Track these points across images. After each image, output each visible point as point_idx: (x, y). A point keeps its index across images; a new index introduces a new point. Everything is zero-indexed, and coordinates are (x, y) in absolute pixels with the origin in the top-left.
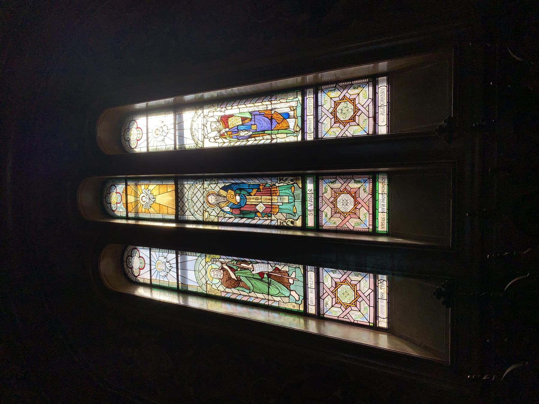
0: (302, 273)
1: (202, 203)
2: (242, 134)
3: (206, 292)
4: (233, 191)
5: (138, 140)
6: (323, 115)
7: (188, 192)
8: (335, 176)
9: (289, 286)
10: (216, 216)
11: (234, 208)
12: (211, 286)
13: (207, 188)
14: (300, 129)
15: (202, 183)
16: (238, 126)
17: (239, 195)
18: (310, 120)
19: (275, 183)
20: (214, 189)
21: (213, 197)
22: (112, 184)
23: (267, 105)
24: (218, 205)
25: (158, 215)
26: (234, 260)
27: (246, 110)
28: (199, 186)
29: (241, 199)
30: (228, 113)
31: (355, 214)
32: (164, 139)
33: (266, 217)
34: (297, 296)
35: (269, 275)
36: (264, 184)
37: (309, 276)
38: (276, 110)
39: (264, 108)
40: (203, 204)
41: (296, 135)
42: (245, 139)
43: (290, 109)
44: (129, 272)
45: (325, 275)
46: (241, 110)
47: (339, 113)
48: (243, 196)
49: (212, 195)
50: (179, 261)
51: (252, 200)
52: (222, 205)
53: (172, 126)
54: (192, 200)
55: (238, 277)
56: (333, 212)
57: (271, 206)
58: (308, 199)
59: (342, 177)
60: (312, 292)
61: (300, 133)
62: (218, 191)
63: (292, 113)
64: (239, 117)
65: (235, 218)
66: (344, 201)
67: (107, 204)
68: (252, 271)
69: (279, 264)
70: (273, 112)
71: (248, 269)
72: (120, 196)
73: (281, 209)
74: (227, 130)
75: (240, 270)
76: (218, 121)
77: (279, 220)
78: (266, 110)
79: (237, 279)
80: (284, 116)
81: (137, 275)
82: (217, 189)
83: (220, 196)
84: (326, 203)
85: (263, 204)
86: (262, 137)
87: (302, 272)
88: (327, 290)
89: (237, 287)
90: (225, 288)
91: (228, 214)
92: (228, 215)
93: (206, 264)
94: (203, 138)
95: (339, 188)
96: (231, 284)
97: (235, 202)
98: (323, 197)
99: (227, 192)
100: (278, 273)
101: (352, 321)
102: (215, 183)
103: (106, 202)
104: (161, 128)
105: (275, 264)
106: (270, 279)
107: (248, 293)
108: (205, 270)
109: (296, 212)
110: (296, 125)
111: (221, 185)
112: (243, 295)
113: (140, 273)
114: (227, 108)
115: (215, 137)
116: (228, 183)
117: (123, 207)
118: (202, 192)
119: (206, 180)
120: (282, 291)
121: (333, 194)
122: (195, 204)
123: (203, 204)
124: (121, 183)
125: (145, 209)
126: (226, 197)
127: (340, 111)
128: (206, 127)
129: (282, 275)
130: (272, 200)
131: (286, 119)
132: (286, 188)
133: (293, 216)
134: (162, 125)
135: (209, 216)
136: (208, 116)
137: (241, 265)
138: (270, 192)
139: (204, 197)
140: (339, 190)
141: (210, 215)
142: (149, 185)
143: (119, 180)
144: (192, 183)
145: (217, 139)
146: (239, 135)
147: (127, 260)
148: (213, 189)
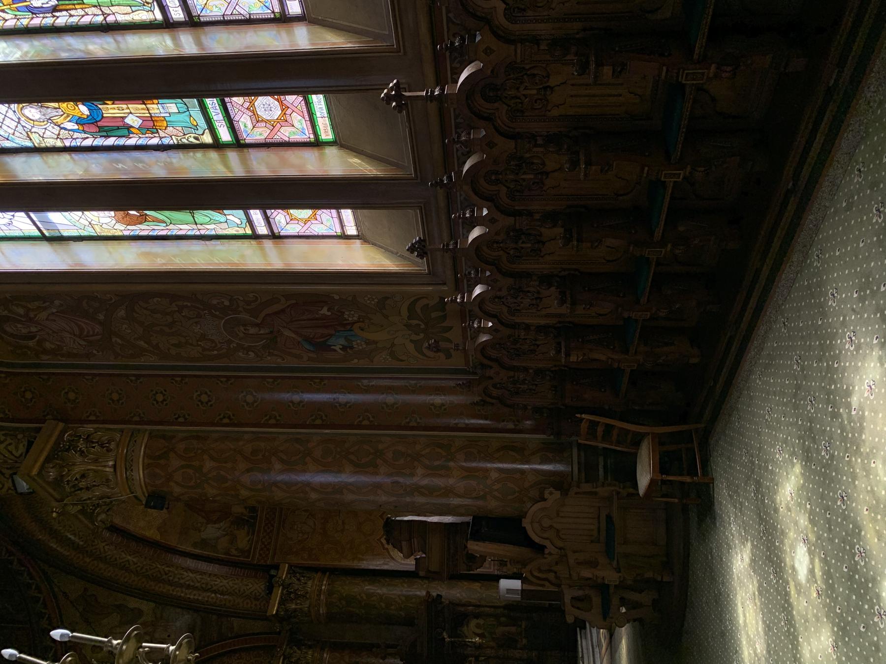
31: (286, 121)
48: (91, 106)
58: (210, 106)
77: (173, 137)
85: (137, 116)
90: (125, 226)
92: (76, 135)
101: (317, 234)
126: (60, 108)
141: (43, 137)
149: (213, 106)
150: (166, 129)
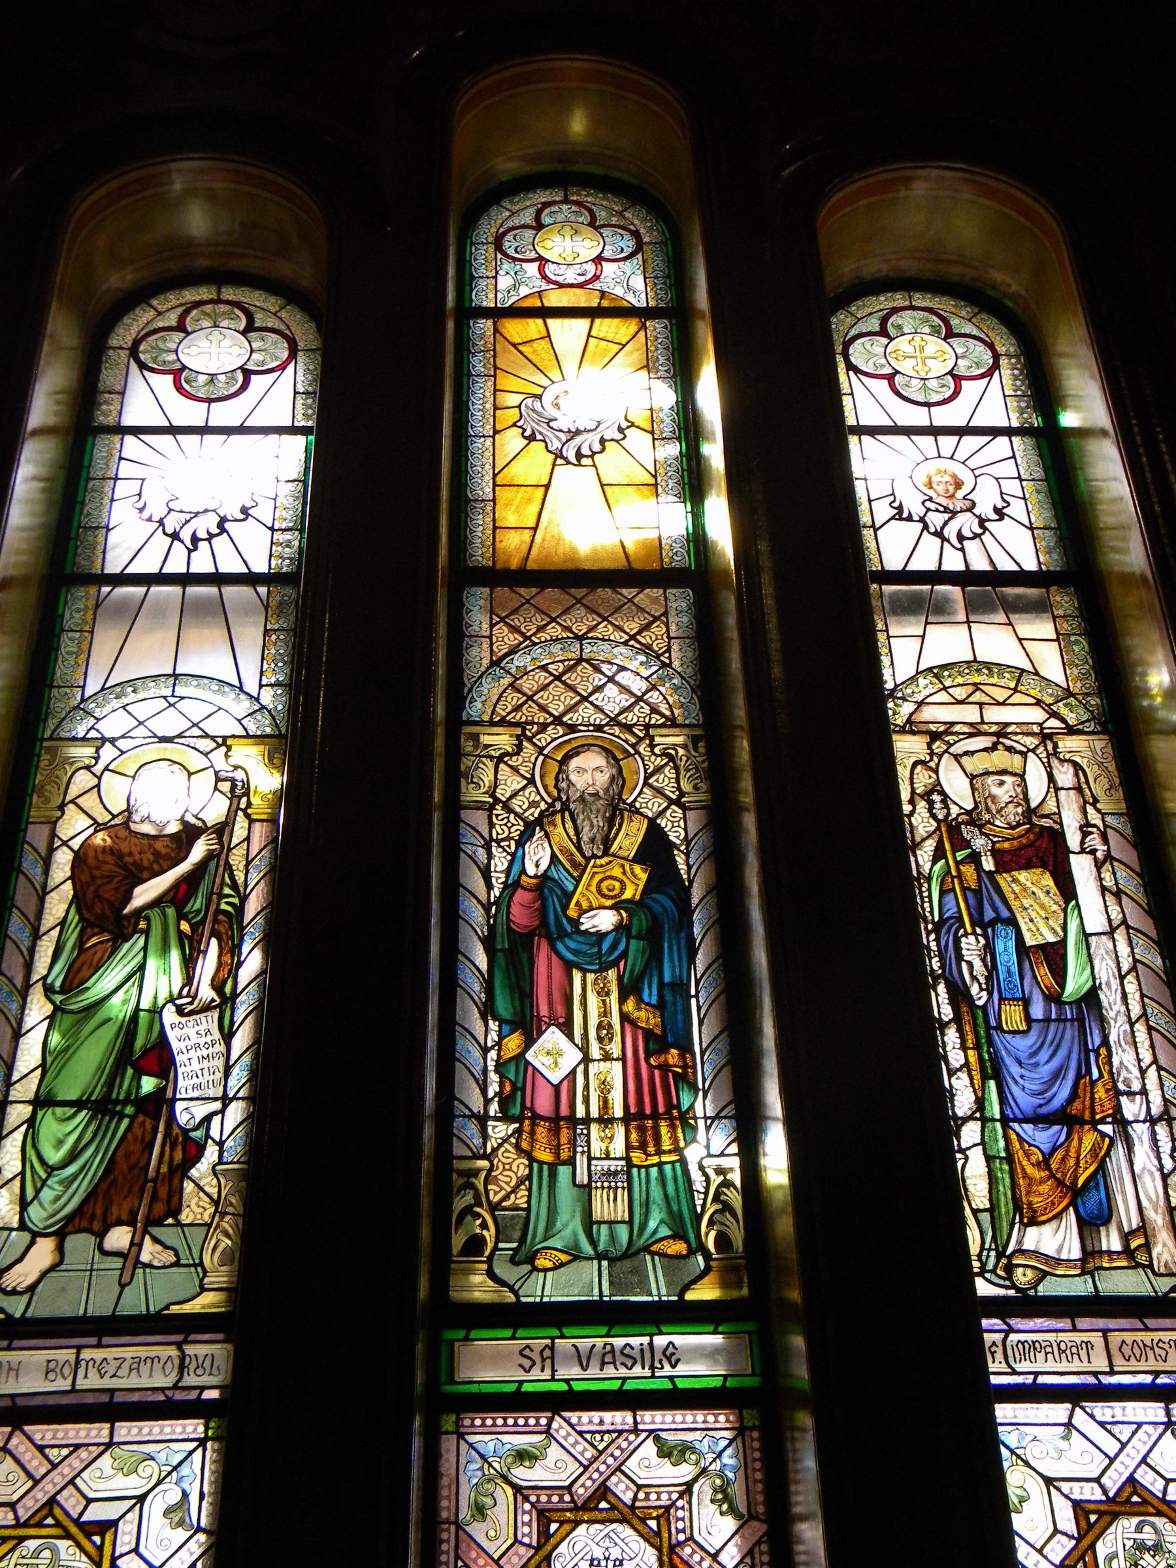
0: (167, 1307)
1: (565, 719)
2: (971, 946)
3: (51, 738)
4: (641, 895)
5: (890, 378)
6: (1116, 1429)
7: (625, 643)
8: (761, 1509)
9: (85, 1224)
10: (493, 795)
11: (542, 898)
12: (88, 768)
13: (652, 746)
14: (1023, 1291)
15: (680, 720)
16: (1013, 922)
17: (619, 927)
18: (1083, 1353)
20: (651, 786)
21: (602, 779)
22: (646, 239)
23: (1144, 1092)
24: (558, 806)
25: (488, 478)
26: (244, 899)
27: (1105, 970)
28: (667, 698)
29: (600, 936)
30: (1081, 868)
32: (909, 519)
33: (501, 1085)
34: (26, 1275)
36: (695, 1073)
37: (152, 1355)
38: (1120, 1150)
39: (1124, 1074)
40: (562, 724)
41: (990, 1266)
42: (942, 967)
43: (1134, 1226)
44: (159, 313)
45: (162, 1457)
46: (1101, 946)
47: (1139, 1529)
49: (614, 771)
50: (229, 591)
51: (593, 1001)
52: (560, 832)
53: (980, 564)
54: (580, 660)
55: (142, 925)
56: (544, 1499)
57: (564, 1118)
58: (619, 1342)
59: (761, 1553)
60: (51, 1376)
61: (1001, 1292)
62: (638, 805)
63: (1112, 1241)
64: (1064, 928)
65: (484, 900)
67: (532, 210)
68: (179, 1002)
69: (220, 1162)
70: (1108, 1129)
71: (189, 980)
72: (581, 279)
73: (553, 1175)
74: (988, 864)
75: (180, 933)
76: (1030, 812)
77: (484, 1164)
78: (1115, 1087)
79: (128, 917)
80: (1092, 1200)
81: (142, 356)
82: (651, 805)
84: (601, 1452)
86: (963, 1061)
87: (175, 1309)
88: (66, 1470)
89: (82, 919)
90: (76, 844)
91: (506, 865)
92: (500, 862)
93: (213, 738)
94: (933, 727)
95: (691, 1538)
96: (99, 882)
97: (578, 904)
98: (632, 1437)
99: (636, 860)
100: (167, 1157)
102: (682, 794)
103: (546, 205)
104: (968, 503)
105: (221, 1144)
106: (129, 1110)
107: (45, 978)
108: (180, 736)
109: (535, 1269)
110: (1049, 1265)
111: (674, 827)
112: (32, 951)
113: (152, 370)
114: (1107, 866)
115: (942, 793)
116: (689, 867)
117: (524, 291)
118: (630, 718)
119: (695, 740)
120: (60, 1183)
121: (653, 1496)
122: (558, 678)
123: (558, 720)
124: (655, 284)
125: (519, 407)
126: (606, 853)
127: (1148, 1536)
128: (993, 748)
129: (154, 1181)
130: (605, 1121)
131: (1073, 1203)
133: (515, 1250)
134: (985, 509)
135: (491, 757)
136: (1055, 763)
138: (648, 1111)
139: (599, 728)
140: (681, 1537)
141: (500, 759)
142: (652, 433)
143: (668, 276)
144: (676, 664)
145: (931, 804)
146: (961, 932)
147: (228, 302)
148: (647, 778)
149: (620, 1359)
150: (517, 1147)
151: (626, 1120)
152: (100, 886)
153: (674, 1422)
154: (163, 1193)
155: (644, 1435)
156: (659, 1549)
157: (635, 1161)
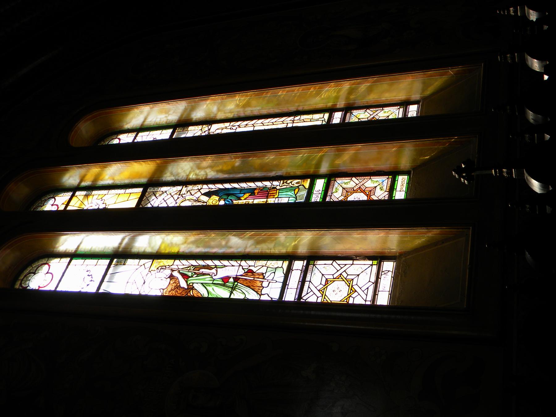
19: (275, 186)
23: (288, 123)
35: (236, 279)
36: (261, 188)
55: (191, 284)
66: (356, 198)
83: (198, 201)
95: (353, 188)
98: (332, 196)
105: (250, 266)
106: (236, 283)
108: (144, 280)
129: (254, 278)
132: (288, 190)
137: (200, 270)
140: (352, 189)
151: (267, 198)
152: (178, 293)
153: (331, 190)
154: (257, 276)
155: (332, 195)
156: (354, 193)
157: (277, 197)
